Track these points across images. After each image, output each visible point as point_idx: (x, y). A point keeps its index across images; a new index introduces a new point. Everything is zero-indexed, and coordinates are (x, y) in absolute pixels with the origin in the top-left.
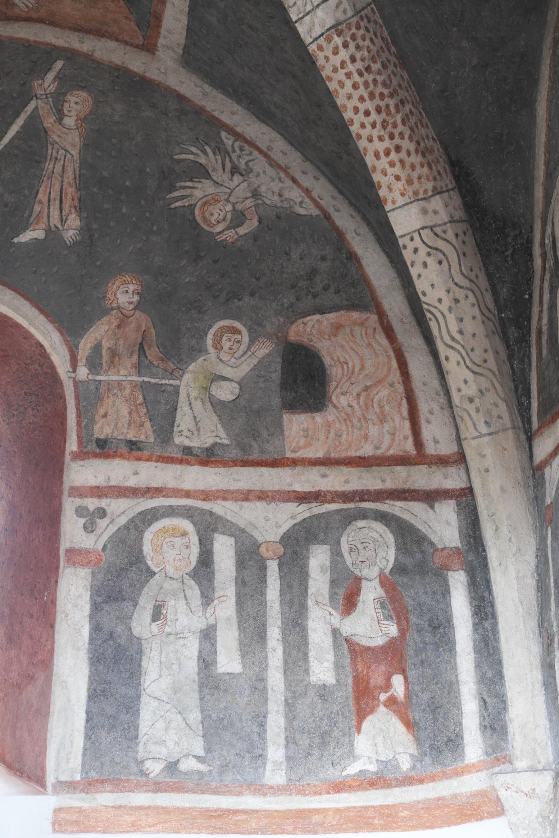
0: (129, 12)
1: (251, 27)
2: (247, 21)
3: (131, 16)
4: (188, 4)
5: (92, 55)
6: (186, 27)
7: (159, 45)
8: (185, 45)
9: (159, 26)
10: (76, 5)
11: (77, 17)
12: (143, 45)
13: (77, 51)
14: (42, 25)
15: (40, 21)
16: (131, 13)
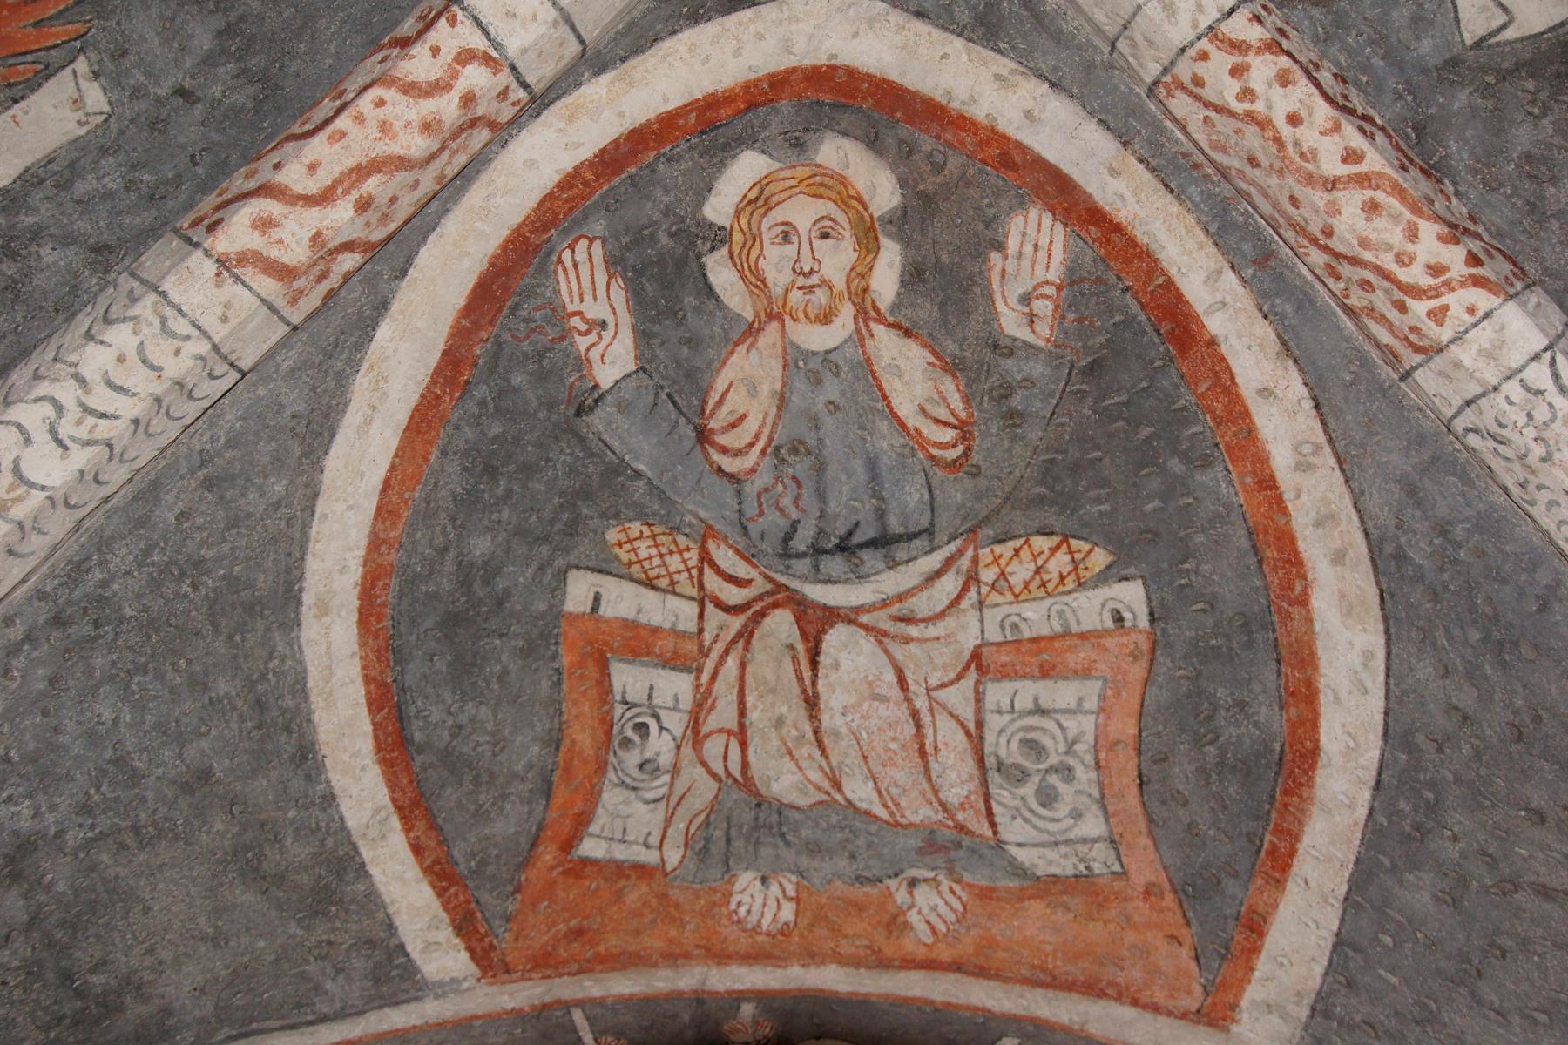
0: (1182, 921)
1: (1544, 892)
2: (1532, 878)
3: (1185, 931)
4: (1347, 874)
5: (1082, 1030)
6: (1331, 940)
7: (1244, 1003)
8: (1319, 993)
9: (1255, 950)
10: (1053, 918)
11: (1049, 948)
12: (1198, 1011)
13: (1046, 1021)
14: (958, 976)
15: (957, 967)
16: (1188, 924)
